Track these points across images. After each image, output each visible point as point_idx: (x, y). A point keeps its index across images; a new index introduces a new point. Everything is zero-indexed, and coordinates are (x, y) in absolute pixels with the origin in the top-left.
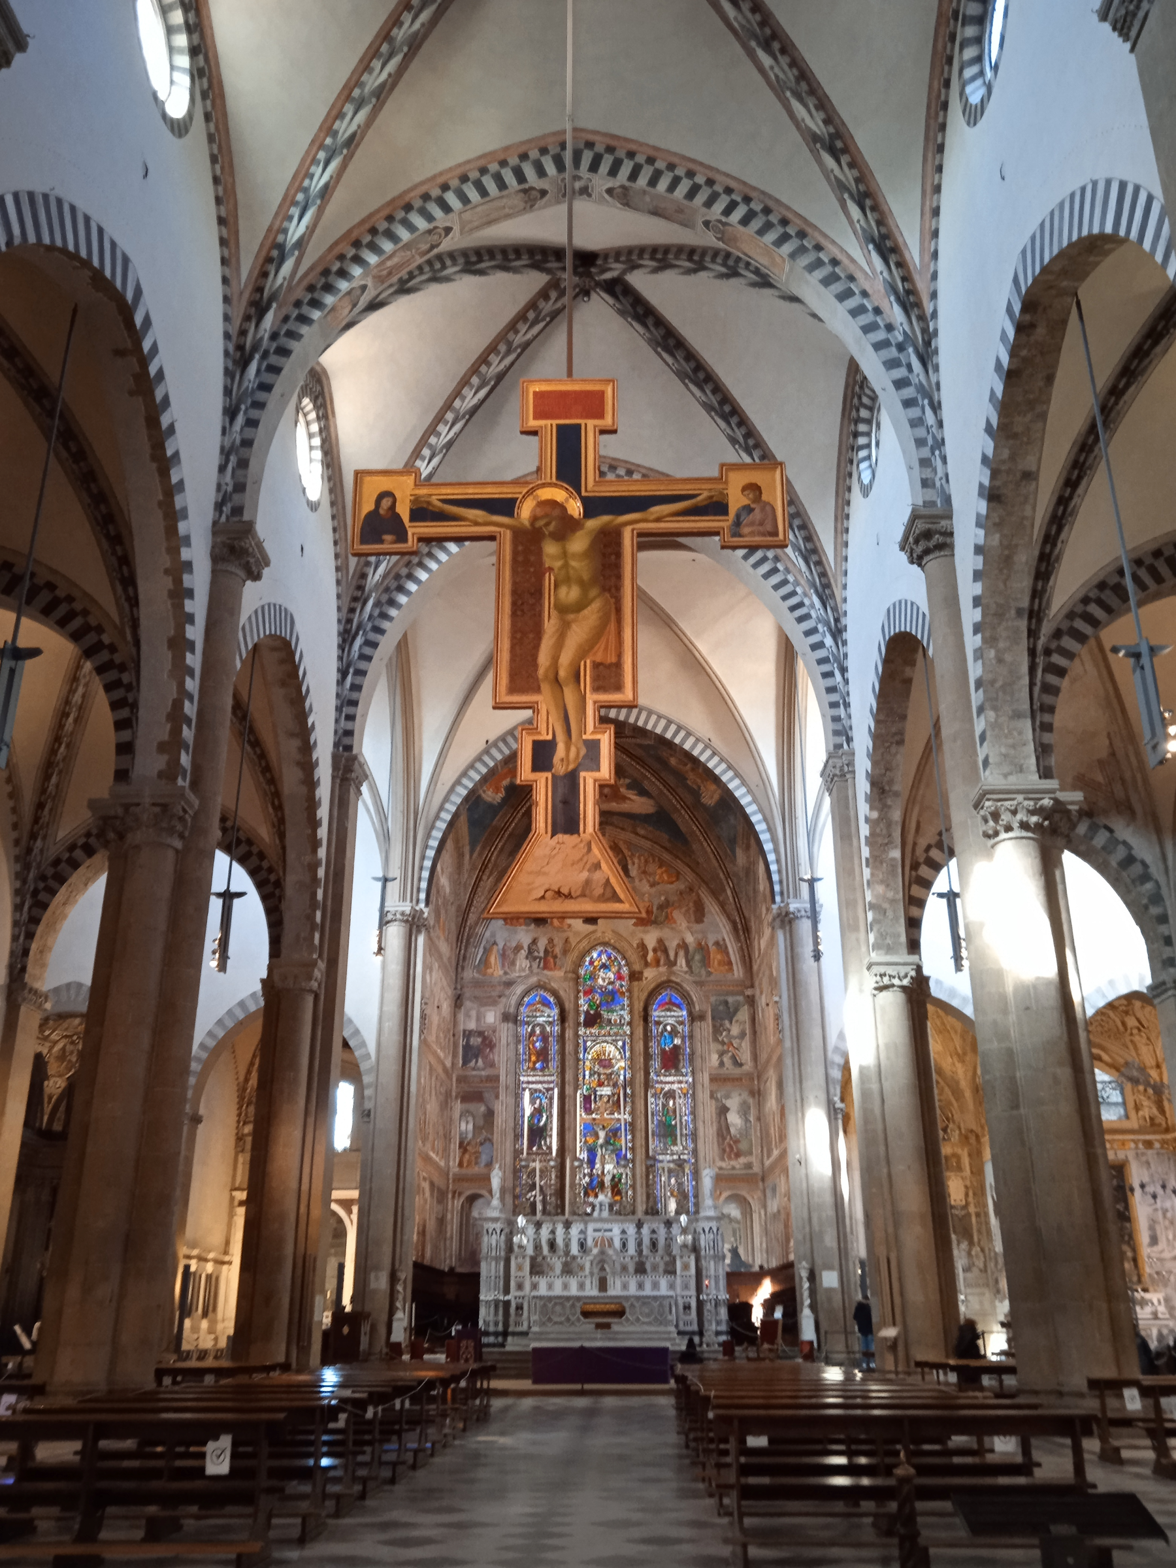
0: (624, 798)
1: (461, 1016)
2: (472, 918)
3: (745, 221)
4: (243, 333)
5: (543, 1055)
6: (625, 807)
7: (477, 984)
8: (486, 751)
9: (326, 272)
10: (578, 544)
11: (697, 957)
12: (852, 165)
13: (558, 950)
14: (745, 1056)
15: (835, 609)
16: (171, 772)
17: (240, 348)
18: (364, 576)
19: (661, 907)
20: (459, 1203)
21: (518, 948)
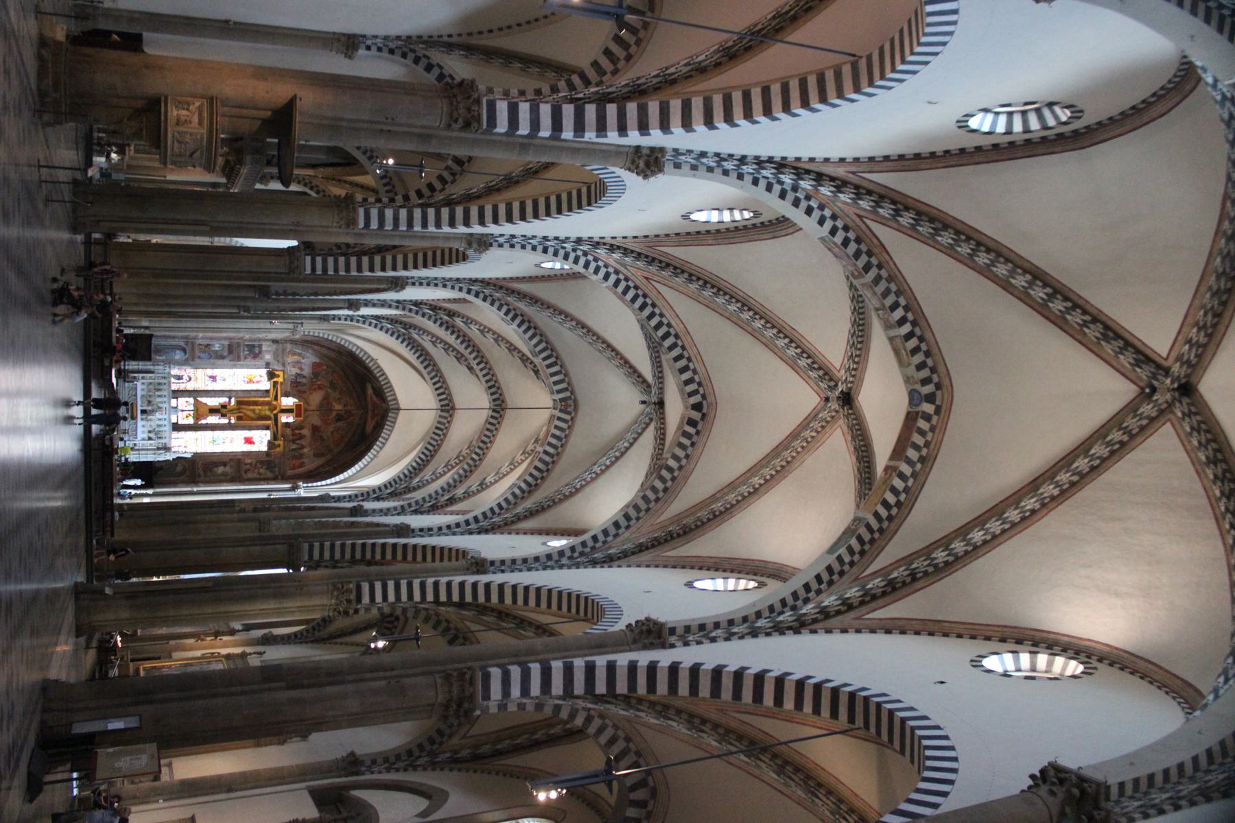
1: (268, 343)
2: (316, 347)
3: (472, 459)
4: (426, 304)
5: (251, 381)
6: (369, 419)
7: (284, 350)
8: (372, 360)
9: (453, 327)
10: (268, 413)
13: (300, 388)
14: (250, 475)
15: (387, 498)
16: (277, 294)
17: (421, 303)
18: (401, 323)
19: (321, 437)
20: (182, 344)
21: (301, 369)
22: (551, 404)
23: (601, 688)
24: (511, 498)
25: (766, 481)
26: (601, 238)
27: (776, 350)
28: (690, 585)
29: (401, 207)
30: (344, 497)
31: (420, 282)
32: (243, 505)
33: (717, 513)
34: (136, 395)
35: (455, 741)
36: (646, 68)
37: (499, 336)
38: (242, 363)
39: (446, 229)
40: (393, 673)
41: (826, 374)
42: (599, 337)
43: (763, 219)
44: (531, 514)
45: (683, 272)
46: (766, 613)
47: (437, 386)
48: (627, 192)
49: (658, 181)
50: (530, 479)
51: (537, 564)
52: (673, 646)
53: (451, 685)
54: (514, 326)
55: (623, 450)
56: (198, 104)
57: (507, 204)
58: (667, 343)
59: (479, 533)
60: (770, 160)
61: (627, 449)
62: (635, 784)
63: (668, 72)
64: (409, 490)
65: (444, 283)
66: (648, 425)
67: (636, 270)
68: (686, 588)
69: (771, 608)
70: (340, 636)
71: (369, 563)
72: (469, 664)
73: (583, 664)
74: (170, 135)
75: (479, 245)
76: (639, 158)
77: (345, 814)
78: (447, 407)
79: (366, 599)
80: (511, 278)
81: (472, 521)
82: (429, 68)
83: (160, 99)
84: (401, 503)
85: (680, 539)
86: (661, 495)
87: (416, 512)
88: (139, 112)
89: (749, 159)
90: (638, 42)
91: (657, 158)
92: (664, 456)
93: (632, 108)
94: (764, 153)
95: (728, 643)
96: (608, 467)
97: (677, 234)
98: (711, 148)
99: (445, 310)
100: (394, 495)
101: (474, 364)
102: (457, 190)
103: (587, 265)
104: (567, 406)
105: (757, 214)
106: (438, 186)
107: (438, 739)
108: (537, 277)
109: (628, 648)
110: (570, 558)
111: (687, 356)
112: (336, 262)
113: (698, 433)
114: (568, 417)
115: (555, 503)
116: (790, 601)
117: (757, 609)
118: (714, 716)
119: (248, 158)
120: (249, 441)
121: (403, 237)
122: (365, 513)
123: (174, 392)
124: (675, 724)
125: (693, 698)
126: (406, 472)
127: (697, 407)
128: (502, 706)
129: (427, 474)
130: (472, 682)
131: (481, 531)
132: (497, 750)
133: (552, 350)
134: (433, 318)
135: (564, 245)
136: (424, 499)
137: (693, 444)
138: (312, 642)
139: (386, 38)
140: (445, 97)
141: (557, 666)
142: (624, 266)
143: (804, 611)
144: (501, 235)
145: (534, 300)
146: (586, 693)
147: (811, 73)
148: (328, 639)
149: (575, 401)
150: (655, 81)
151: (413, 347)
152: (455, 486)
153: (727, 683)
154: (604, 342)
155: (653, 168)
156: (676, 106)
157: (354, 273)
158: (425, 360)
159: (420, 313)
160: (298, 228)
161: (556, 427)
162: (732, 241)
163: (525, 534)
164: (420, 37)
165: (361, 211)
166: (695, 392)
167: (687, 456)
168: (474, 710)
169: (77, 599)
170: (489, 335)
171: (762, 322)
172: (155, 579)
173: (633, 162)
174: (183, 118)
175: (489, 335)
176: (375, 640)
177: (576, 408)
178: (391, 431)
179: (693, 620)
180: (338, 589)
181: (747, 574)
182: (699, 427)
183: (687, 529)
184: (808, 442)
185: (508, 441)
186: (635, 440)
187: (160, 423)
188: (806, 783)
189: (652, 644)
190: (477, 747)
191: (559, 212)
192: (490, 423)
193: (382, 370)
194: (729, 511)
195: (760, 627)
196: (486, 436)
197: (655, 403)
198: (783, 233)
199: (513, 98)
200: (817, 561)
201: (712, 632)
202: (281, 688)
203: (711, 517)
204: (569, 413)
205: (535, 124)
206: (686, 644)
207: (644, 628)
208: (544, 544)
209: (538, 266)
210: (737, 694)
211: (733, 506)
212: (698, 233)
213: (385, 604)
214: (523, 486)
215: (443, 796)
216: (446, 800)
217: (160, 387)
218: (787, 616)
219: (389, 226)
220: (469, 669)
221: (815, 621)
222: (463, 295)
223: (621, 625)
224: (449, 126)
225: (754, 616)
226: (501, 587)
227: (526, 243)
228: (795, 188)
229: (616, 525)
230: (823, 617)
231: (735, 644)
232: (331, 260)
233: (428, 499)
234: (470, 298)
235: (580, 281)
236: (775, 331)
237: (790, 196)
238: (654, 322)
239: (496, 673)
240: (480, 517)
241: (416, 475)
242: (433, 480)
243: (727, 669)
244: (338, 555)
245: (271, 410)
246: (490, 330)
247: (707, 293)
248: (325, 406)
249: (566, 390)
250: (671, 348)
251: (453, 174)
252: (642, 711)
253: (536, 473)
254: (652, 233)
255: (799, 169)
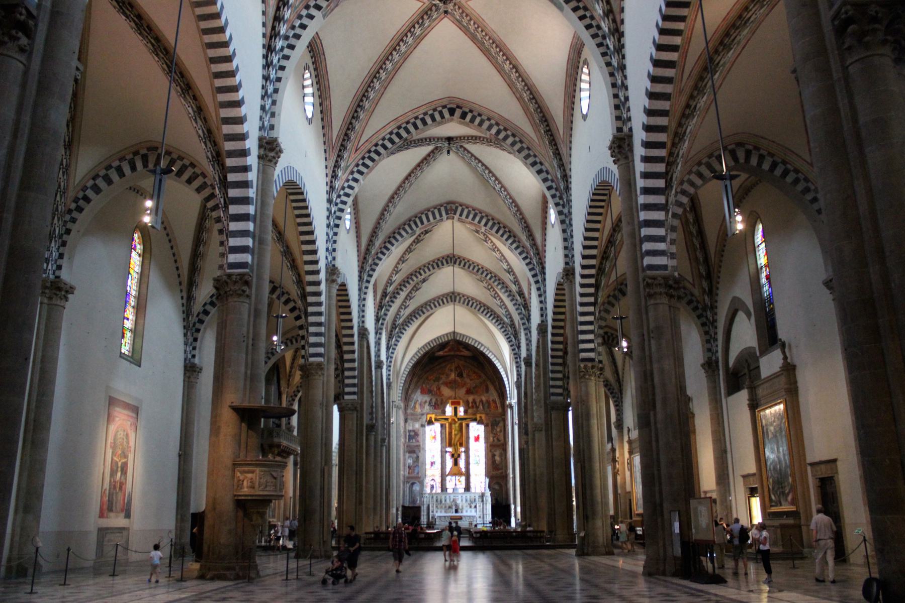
0: (461, 351)
2: (410, 392)
3: (490, 279)
4: (378, 313)
5: (434, 438)
6: (462, 354)
7: (412, 414)
8: (418, 351)
9: (394, 293)
10: (457, 425)
11: (486, 405)
12: (513, 275)
14: (502, 438)
15: (518, 341)
16: (372, 419)
17: (377, 317)
19: (474, 388)
20: (408, 485)
21: (426, 402)
22: (450, 221)
23: (660, 183)
24: (519, 251)
25: (507, 59)
26: (327, 185)
27: (409, 52)
28: (585, 117)
29: (307, 331)
30: (517, 371)
31: (362, 317)
32: (523, 442)
33: (531, 96)
34: (445, 517)
35: (696, 292)
36: (200, 152)
37: (400, 259)
38: (421, 444)
39: (323, 298)
40: (646, 333)
41: (426, 13)
42: (400, 186)
43: (310, 64)
44: (531, 236)
45: (351, 123)
46: (608, 58)
47: (437, 305)
48: (292, 166)
49: (284, 141)
50: (505, 236)
51: (568, 231)
52: (631, 129)
53: (655, 293)
54: (393, 248)
55: (484, 168)
56: (239, 474)
57: (304, 254)
58: (404, 135)
59: (544, 274)
60: (265, 57)
61: (483, 164)
62: (733, 158)
63: (202, 135)
64: (513, 325)
65: (362, 300)
66: (465, 149)
67: (350, 158)
68: (587, 120)
69: (604, 54)
70: (618, 374)
71: (566, 353)
72: (641, 280)
73: (642, 196)
74: (261, 493)
75: (334, 274)
76: (267, 156)
77: (746, 371)
78: (452, 297)
79: (592, 355)
80: (358, 251)
81: (535, 279)
82: (206, 313)
83: (236, 500)
84: (522, 330)
85: (550, 124)
86: (517, 139)
87: (529, 320)
88: (247, 515)
89: (265, 73)
90: (181, 158)
91: (267, 143)
92: (488, 136)
93: (230, 162)
94: (261, 62)
95: (629, 88)
96: (497, 179)
97: (323, 128)
98: (258, 102)
99: (382, 299)
100: (516, 335)
101: (421, 278)
102: (294, 291)
103: (347, 195)
104: (451, 209)
105: (306, 68)
106: (291, 305)
107: (695, 304)
108: (357, 232)
109: (631, 164)
110: (564, 206)
111: (413, 120)
112: (349, 377)
113: (471, 111)
114: (460, 209)
115: (523, 218)
116: (599, 40)
117: (604, 65)
118: (683, 99)
119: (276, 440)
120: (477, 439)
121: (329, 329)
122: (529, 356)
123: (442, 490)
124: (689, 128)
125: (670, 114)
126: (500, 327)
127: (452, 112)
128: (672, 256)
129: (501, 312)
130: (654, 278)
131: (543, 272)
132: (703, 261)
133: (410, 221)
134: (388, 308)
135: (333, 212)
136: (519, 314)
137: (480, 115)
138: (621, 394)
139: (186, 344)
140: (227, 300)
141: (643, 216)
142: (347, 167)
143: (606, 29)
144: (327, 258)
145: (374, 234)
146: (664, 194)
147: (198, 26)
148: (619, 383)
149: (448, 203)
150: (209, 145)
151: (409, 322)
152: (510, 291)
153: (660, 88)
154: (404, 182)
155: (275, 146)
156: (227, 129)
157: (356, 364)
158: (418, 313)
159: (384, 317)
160: (325, 404)
161: (467, 217)
162: (327, 85)
163: (545, 240)
164: (184, 319)
165: (312, 359)
166: (441, 113)
167: (489, 119)
168: (674, 278)
169: (588, 554)
170: (400, 267)
171: (387, 62)
172: (574, 503)
173: (270, 161)
174: (249, 484)
175: (400, 267)
176: (621, 348)
177: (453, 203)
178: (470, 338)
179: (611, 114)
180: (584, 375)
181: (577, 73)
182: (467, 110)
183: (543, 118)
184: (478, 27)
185: (478, 253)
186: (476, 158)
187: (464, 500)
188: (738, 28)
189: (629, 145)
190: (701, 276)
191: (308, 216)
192: (464, 266)
193: (426, 345)
194: (530, 88)
195: (618, 64)
196: (473, 269)
197: (449, 144)
198: (320, 47)
199: (226, 250)
200: (566, 16)
201: (620, 100)
202: (655, 415)
203: (534, 101)
204: (457, 208)
205: (244, 233)
206: (629, 119)
207: (616, 151)
208: (553, 226)
209: (348, 231)
210: (668, 80)
211: (526, 85)
212: (322, 112)
213: (595, 341)
214: (510, 241)
215: (736, 300)
216: (737, 298)
217: (439, 500)
218: (610, 43)
219: (322, 340)
220: (644, 280)
221: (614, 21)
222: (371, 286)
223: (614, 168)
224: (248, 296)
225: (610, 68)
226: (584, 257)
227: (332, 240)
228: (286, 38)
229: (539, 172)
230: (611, 15)
231: (630, 82)
232: (347, 381)
233: (519, 311)
234: (373, 280)
235: (360, 200)
236: (394, 53)
237: (292, 41)
238: (389, 145)
239: (647, 261)
240: (533, 273)
241: (502, 320)
242: (506, 307)
243: (649, 88)
244: (560, 375)
245: (455, 422)
246: (396, 267)
247: (367, 104)
248: (452, 385)
249: (439, 210)
250: (408, 132)
251: (283, 294)
252: (678, 152)
253: (501, 232)
254: (323, 147)
255: (272, 35)
